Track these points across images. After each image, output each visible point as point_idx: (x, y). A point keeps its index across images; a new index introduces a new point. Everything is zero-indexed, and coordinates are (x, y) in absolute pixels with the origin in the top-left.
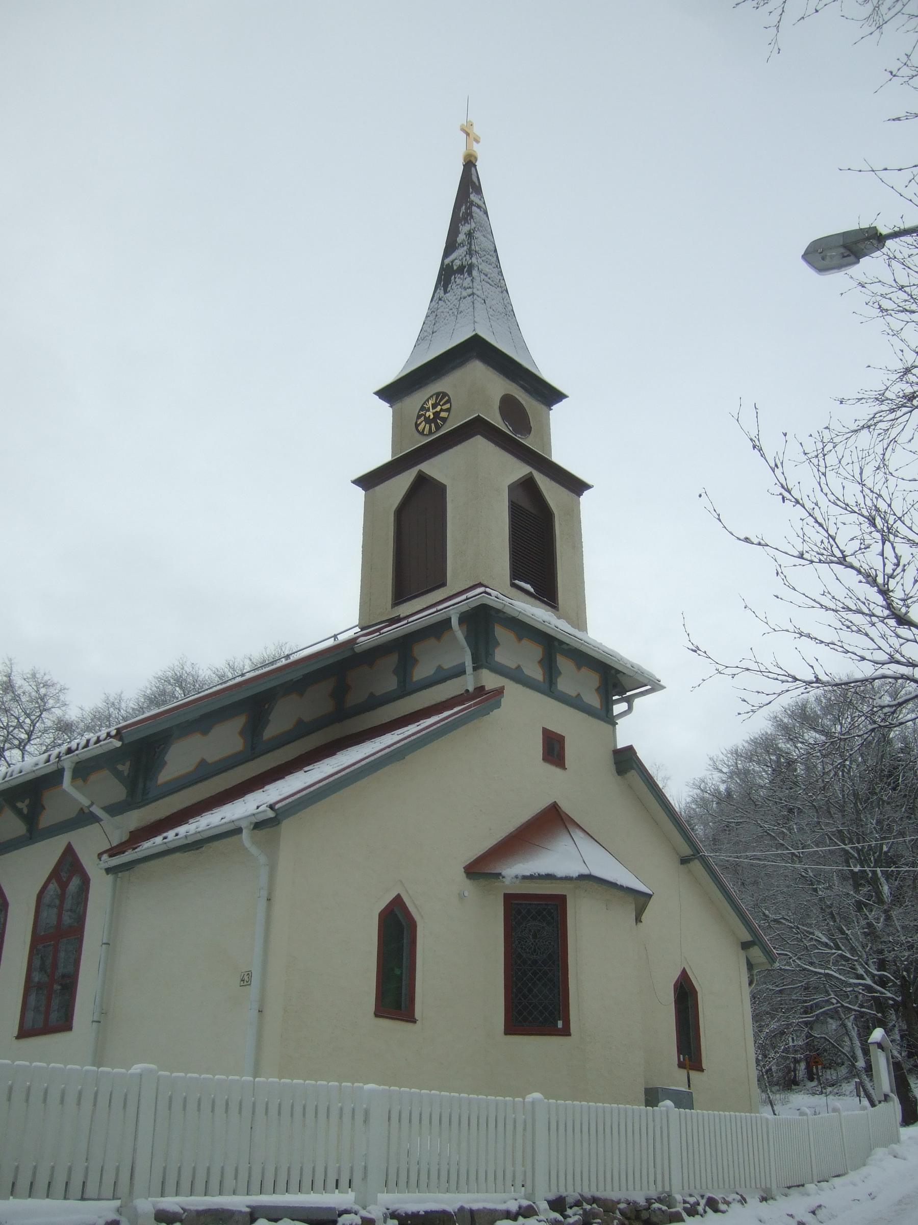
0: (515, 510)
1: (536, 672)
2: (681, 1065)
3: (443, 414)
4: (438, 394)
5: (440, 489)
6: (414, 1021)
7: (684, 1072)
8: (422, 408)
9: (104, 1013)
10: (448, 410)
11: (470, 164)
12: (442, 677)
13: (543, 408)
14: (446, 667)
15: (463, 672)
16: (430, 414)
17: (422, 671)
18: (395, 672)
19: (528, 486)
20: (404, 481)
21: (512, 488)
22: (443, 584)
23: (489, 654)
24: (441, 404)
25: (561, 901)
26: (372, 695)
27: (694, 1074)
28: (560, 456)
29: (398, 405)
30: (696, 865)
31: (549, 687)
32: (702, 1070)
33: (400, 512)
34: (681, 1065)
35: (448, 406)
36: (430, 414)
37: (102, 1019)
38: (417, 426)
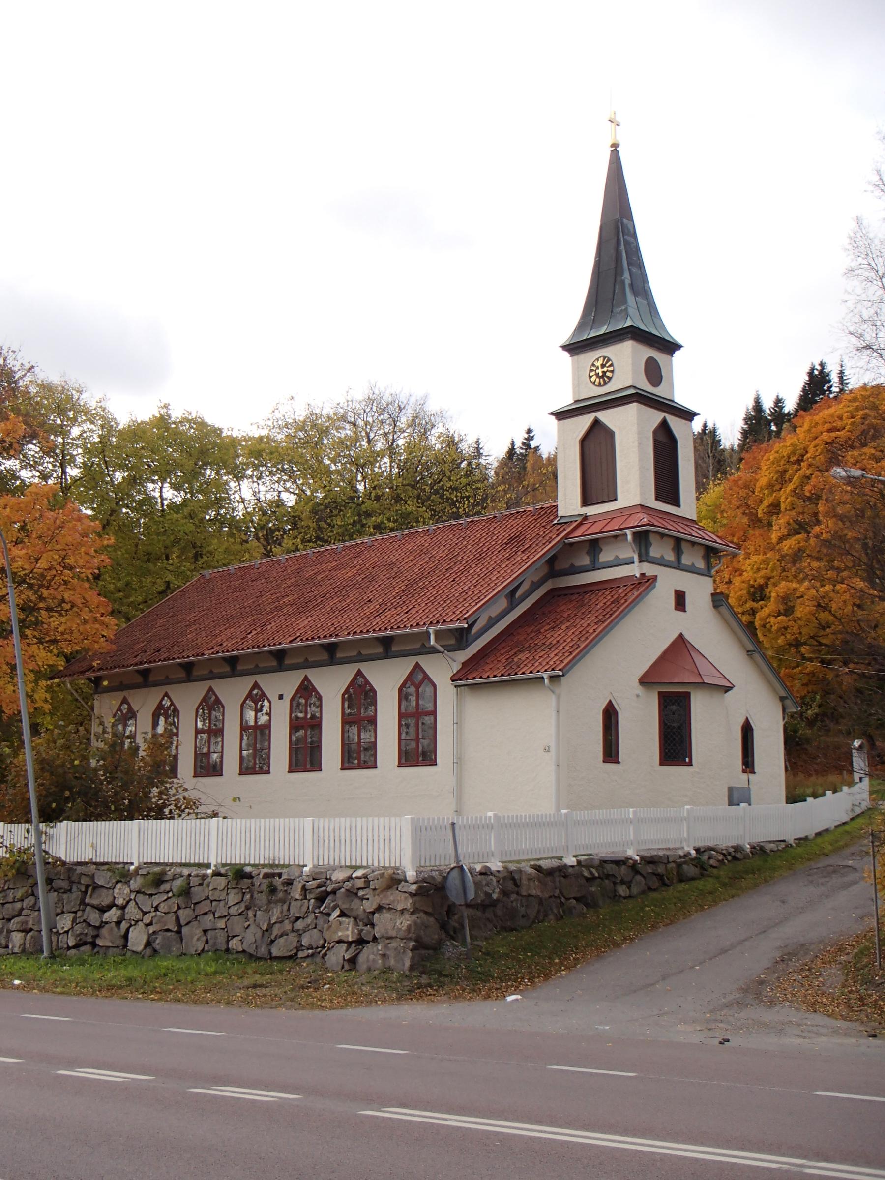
1: (670, 557)
2: (744, 771)
3: (608, 374)
4: (604, 357)
5: (610, 434)
6: (619, 762)
7: (745, 776)
8: (593, 365)
9: (460, 758)
10: (612, 372)
11: (615, 146)
12: (619, 563)
13: (669, 357)
14: (621, 557)
16: (600, 371)
17: (605, 557)
18: (588, 553)
19: (664, 424)
20: (585, 421)
21: (655, 432)
22: (616, 500)
23: (647, 553)
24: (607, 365)
25: (687, 695)
26: (572, 565)
27: (751, 776)
28: (682, 397)
29: (576, 357)
30: (757, 656)
31: (678, 565)
33: (583, 441)
34: (744, 771)
35: (611, 369)
36: (600, 371)
37: (459, 762)
38: (590, 377)
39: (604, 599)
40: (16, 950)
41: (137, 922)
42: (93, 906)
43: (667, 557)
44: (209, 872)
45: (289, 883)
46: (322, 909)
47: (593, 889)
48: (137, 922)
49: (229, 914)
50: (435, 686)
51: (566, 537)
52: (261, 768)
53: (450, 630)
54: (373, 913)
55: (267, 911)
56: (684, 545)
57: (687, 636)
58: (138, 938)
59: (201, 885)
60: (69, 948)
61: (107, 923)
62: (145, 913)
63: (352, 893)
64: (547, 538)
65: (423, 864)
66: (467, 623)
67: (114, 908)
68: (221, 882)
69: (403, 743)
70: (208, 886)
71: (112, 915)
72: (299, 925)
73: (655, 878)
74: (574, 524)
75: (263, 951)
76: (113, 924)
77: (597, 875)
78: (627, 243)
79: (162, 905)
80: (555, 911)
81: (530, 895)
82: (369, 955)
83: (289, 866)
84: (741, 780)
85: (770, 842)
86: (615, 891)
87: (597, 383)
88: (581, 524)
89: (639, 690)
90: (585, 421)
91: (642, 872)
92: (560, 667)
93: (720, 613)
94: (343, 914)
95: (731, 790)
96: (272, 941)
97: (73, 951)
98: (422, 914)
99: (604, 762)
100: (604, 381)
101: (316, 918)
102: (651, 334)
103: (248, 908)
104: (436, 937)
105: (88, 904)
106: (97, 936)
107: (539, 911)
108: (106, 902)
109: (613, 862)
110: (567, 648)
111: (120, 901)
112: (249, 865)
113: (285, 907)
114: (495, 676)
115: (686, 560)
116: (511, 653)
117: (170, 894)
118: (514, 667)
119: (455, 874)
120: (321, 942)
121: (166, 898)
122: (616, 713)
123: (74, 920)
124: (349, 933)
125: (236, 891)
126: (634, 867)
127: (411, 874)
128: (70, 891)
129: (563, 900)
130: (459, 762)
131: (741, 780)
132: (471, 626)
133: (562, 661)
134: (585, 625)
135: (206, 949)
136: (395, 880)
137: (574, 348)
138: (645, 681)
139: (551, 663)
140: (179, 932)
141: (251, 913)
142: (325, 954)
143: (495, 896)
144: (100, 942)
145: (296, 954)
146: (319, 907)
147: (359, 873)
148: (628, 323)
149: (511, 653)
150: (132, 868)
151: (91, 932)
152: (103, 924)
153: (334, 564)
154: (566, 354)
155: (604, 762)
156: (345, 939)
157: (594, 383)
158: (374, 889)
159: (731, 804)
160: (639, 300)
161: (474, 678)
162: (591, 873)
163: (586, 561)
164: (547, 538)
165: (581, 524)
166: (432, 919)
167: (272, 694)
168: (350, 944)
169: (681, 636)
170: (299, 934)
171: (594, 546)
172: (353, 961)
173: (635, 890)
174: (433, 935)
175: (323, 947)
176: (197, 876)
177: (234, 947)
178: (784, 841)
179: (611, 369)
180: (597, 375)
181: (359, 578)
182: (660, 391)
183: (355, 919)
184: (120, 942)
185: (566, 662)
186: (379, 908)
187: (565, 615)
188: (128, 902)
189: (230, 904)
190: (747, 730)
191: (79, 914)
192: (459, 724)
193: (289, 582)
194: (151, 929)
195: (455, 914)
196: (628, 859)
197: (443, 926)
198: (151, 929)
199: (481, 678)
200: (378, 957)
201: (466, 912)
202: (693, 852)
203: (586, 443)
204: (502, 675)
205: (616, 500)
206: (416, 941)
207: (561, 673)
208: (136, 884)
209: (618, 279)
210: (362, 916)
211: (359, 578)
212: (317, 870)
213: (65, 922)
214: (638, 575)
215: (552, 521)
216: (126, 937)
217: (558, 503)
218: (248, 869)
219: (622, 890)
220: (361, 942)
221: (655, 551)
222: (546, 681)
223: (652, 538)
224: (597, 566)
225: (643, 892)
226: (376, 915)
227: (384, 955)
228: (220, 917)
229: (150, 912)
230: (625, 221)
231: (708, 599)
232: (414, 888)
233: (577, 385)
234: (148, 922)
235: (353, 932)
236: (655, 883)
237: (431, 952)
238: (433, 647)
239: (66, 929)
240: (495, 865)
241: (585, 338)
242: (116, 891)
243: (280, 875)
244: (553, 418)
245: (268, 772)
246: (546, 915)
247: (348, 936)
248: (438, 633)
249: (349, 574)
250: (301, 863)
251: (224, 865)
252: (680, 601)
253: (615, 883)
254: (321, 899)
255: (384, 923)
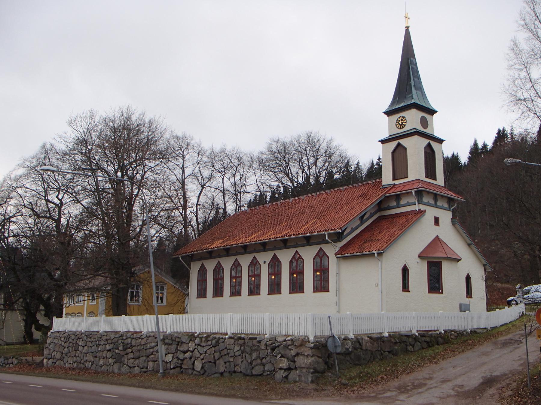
0: (426, 153)
2: (467, 297)
3: (404, 123)
4: (402, 117)
5: (405, 149)
6: (409, 292)
8: (397, 120)
9: (339, 289)
10: (406, 122)
12: (408, 204)
13: (431, 116)
14: (410, 202)
15: (415, 204)
16: (400, 122)
17: (403, 202)
19: (429, 145)
20: (394, 144)
21: (425, 148)
22: (407, 177)
26: (389, 206)
27: (470, 299)
28: (437, 133)
29: (390, 117)
31: (436, 206)
32: (472, 298)
33: (393, 152)
34: (467, 297)
35: (405, 121)
36: (400, 122)
37: (338, 290)
38: (396, 125)
39: (402, 220)
40: (150, 369)
41: (198, 358)
42: (181, 351)
43: (430, 202)
44: (227, 336)
45: (260, 342)
46: (273, 354)
47: (396, 347)
48: (198, 358)
49: (235, 355)
50: (328, 257)
51: (386, 193)
52: (257, 292)
53: (335, 233)
54: (295, 356)
55: (250, 354)
56: (438, 198)
57: (440, 237)
58: (198, 365)
59: (223, 342)
60: (171, 369)
61: (186, 358)
62: (201, 354)
63: (286, 347)
64: (377, 194)
65: (317, 335)
66: (341, 230)
67: (189, 352)
68: (232, 341)
69: (315, 282)
70: (226, 343)
71: (188, 355)
72: (264, 361)
73: (425, 343)
74: (389, 188)
75: (249, 372)
76: (188, 359)
77: (398, 341)
78: (412, 68)
79: (208, 351)
80: (379, 357)
81: (367, 350)
82: (293, 375)
83: (259, 334)
84: (465, 300)
85: (480, 328)
86: (407, 348)
87: (399, 127)
88: (392, 188)
89: (418, 260)
90: (394, 144)
91: (420, 341)
92: (382, 249)
93: (455, 227)
94: (282, 356)
95: (461, 305)
96: (253, 368)
97: (172, 371)
98: (316, 357)
99: (402, 291)
100: (402, 126)
101: (271, 357)
102: (423, 106)
103: (242, 353)
104: (323, 367)
105: (179, 350)
106: (182, 364)
107: (371, 357)
108: (186, 349)
109: (405, 336)
110: (385, 241)
111: (191, 349)
112: (243, 334)
113: (258, 353)
114: (354, 253)
115: (439, 203)
116: (361, 243)
117: (211, 346)
118: (362, 249)
119: (330, 340)
120: (273, 369)
121: (209, 348)
122: (408, 270)
123: (173, 357)
124: (285, 365)
125: (238, 345)
126: (415, 338)
127: (312, 339)
128: (172, 344)
129: (382, 352)
130: (338, 290)
131: (465, 300)
132: (343, 232)
133: (383, 247)
134: (394, 231)
135: (226, 370)
136: (304, 342)
137: (389, 113)
138: (421, 256)
139: (378, 247)
140: (215, 363)
141: (244, 355)
142: (275, 374)
143: (350, 350)
144: (183, 366)
145: (262, 374)
146: (273, 353)
147: (289, 338)
148: (413, 102)
149: (361, 243)
150: (196, 334)
151: (180, 362)
152: (185, 358)
153: (288, 207)
154: (386, 116)
155: (402, 291)
156: (283, 368)
157: (398, 128)
158: (295, 346)
159: (461, 311)
160: (418, 92)
161: (345, 254)
162: (396, 340)
163: (394, 204)
164: (377, 194)
165: (392, 188)
166: (321, 360)
167: (261, 262)
168: (285, 370)
169: (437, 236)
170: (264, 365)
171: (398, 197)
172: (286, 377)
173: (416, 348)
174: (322, 367)
175: (274, 371)
176: (222, 338)
177: (237, 370)
178: (485, 328)
179: (405, 121)
180: (399, 124)
181: (298, 212)
182: (428, 131)
183: (287, 359)
184: (191, 367)
185: (385, 246)
186: (297, 354)
187: (385, 227)
188: (194, 349)
189: (235, 350)
190: (468, 279)
191: (175, 354)
192: (338, 274)
193: (269, 215)
194: (204, 361)
195: (332, 358)
196: (412, 335)
197: (326, 363)
198: (204, 361)
199: (348, 254)
200: (297, 376)
201: (335, 356)
202: (443, 332)
203: (395, 154)
204: (357, 253)
205: (407, 177)
206: (313, 369)
207: (382, 252)
208: (197, 341)
209: (408, 83)
210: (290, 357)
211: (298, 212)
212: (272, 336)
213: (169, 358)
214: (417, 210)
215: (380, 187)
216: (193, 364)
217: (383, 180)
218: (243, 336)
219: (410, 348)
220: (289, 369)
221: (425, 200)
222: (376, 255)
223: (424, 193)
224: (399, 206)
225: (420, 349)
226: (296, 357)
227: (299, 376)
228: (231, 357)
229: (203, 354)
230: (412, 59)
231: (450, 220)
232: (312, 345)
233: (390, 130)
234: (202, 358)
235: (286, 364)
236: (425, 345)
237: (320, 374)
238: (327, 241)
239: (170, 361)
240: (351, 336)
241: (394, 108)
242: (190, 344)
243: (256, 338)
244: (380, 143)
245: (259, 294)
246: (374, 359)
247: (284, 366)
248: (328, 234)
249: (294, 211)
250: (264, 333)
251: (233, 334)
252: (437, 221)
253: (406, 345)
254: (273, 349)
255: (301, 361)
